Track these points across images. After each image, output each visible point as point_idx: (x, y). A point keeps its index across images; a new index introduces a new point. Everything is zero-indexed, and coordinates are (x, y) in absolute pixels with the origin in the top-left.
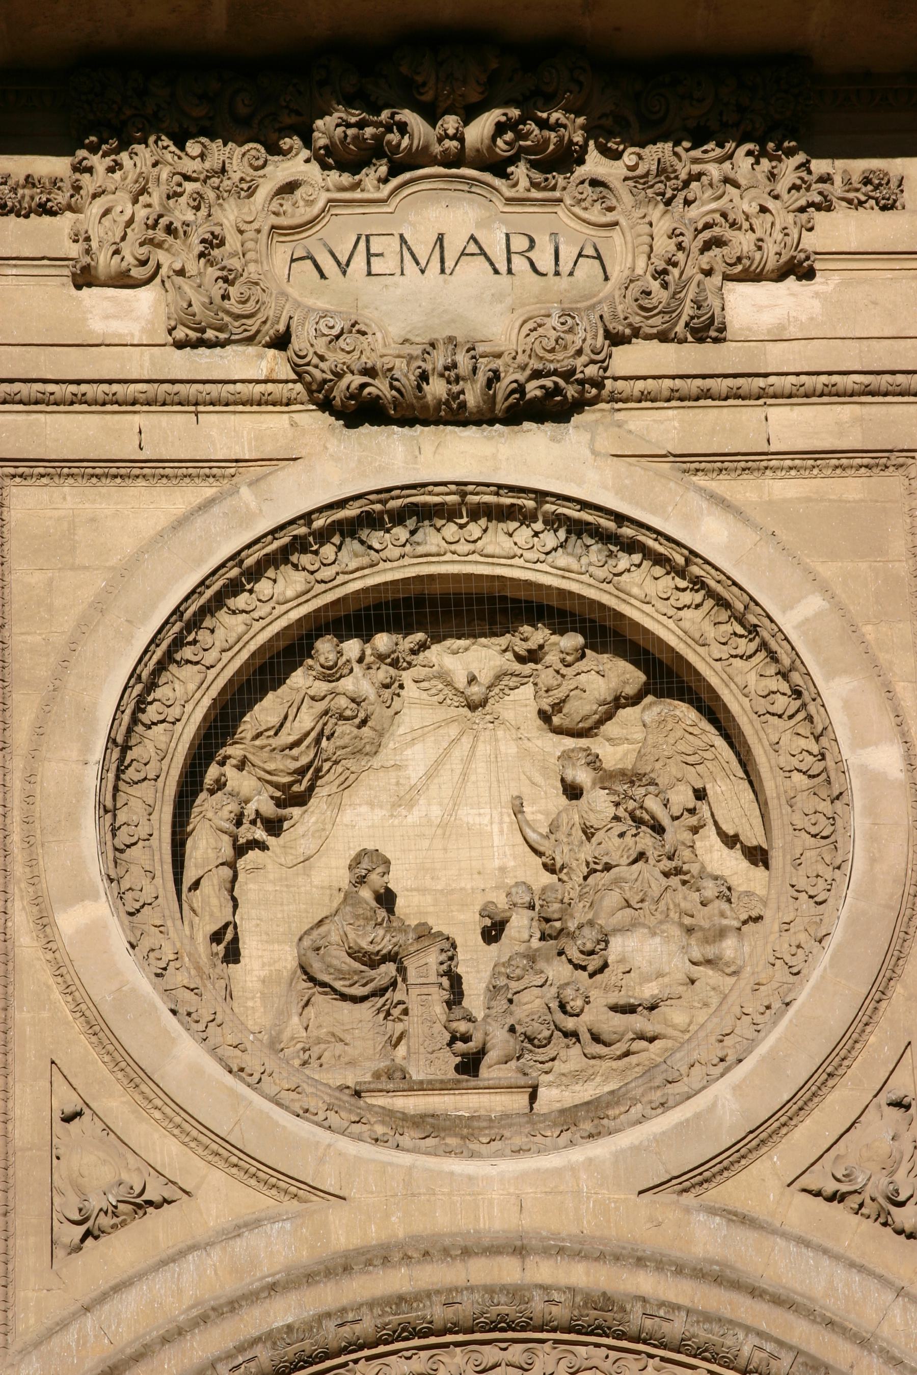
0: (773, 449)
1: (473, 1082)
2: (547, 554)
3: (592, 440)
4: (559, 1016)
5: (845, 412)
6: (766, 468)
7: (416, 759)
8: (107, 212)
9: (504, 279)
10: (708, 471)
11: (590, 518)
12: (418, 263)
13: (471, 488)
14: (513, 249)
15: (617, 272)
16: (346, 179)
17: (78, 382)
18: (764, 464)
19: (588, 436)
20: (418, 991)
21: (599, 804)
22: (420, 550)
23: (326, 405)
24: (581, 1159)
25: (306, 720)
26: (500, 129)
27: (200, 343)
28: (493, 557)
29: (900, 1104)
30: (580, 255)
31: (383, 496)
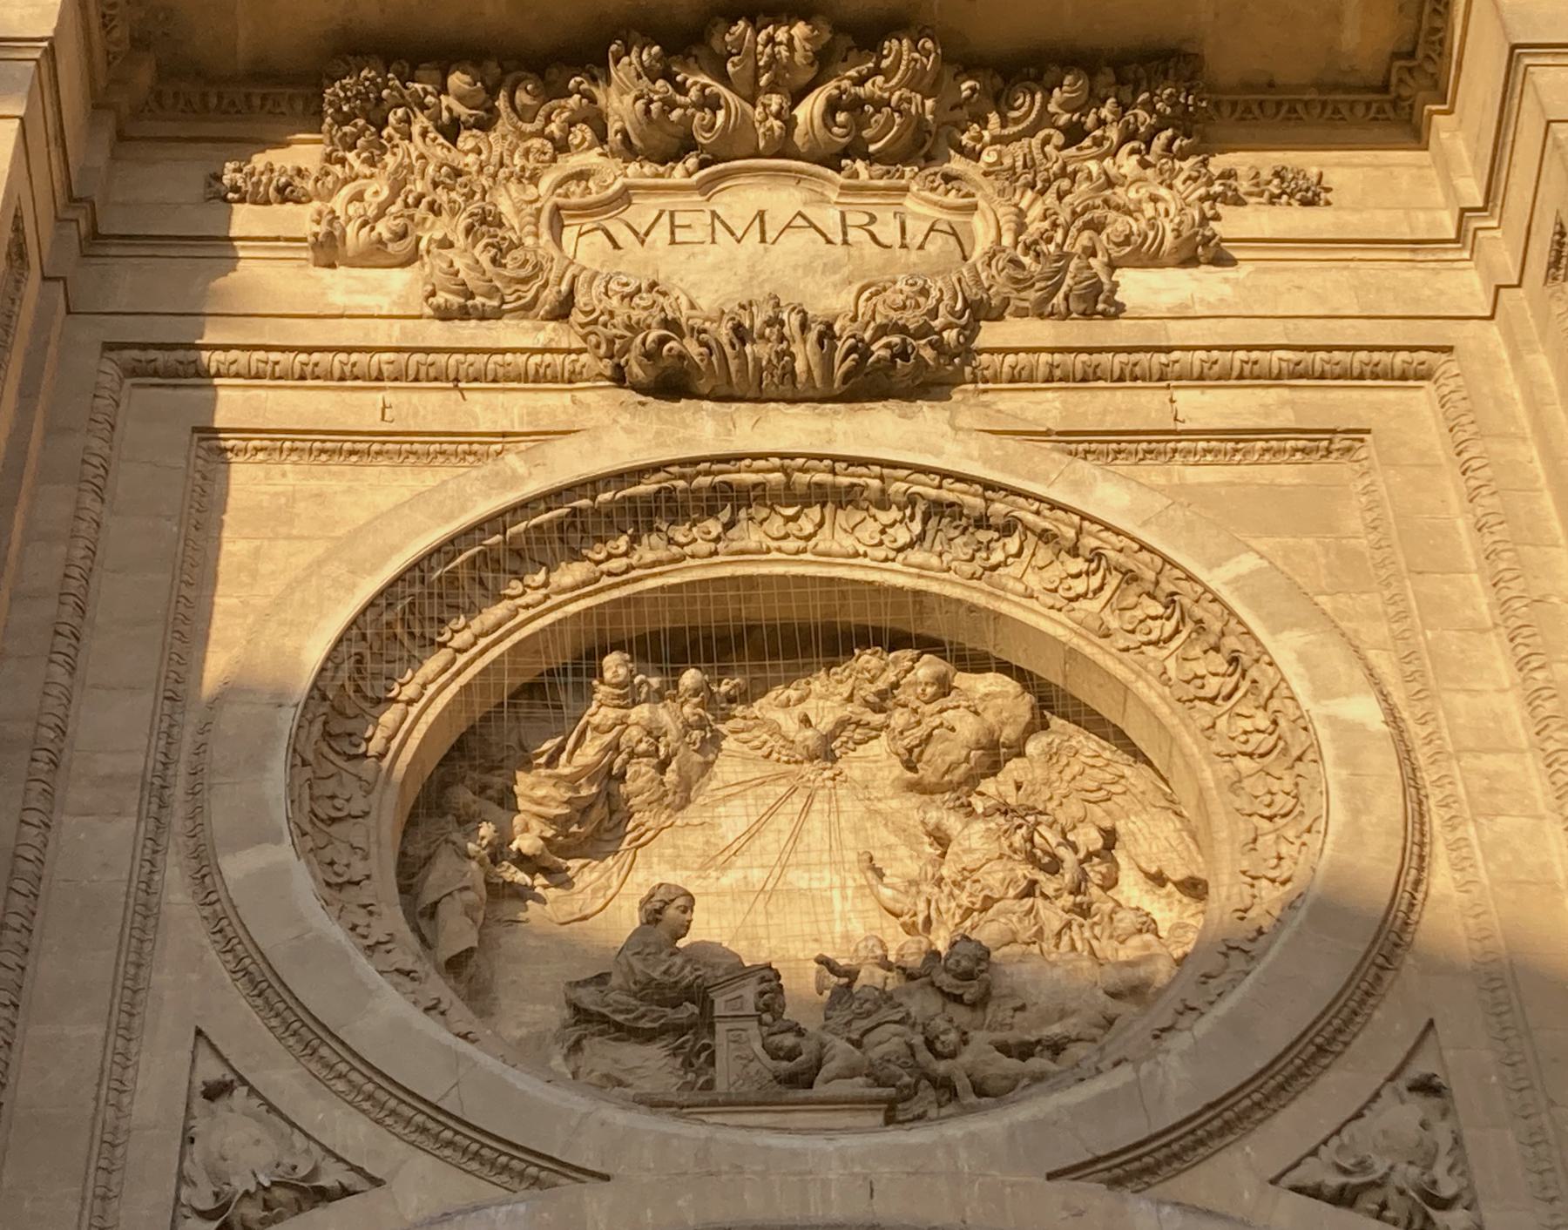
0: (1180, 427)
1: (802, 1094)
2: (900, 550)
3: (952, 416)
4: (924, 1056)
5: (1272, 396)
6: (1175, 451)
7: (733, 820)
8: (358, 197)
9: (839, 251)
10: (1101, 453)
11: (951, 497)
12: (732, 234)
13: (800, 461)
14: (848, 222)
15: (977, 255)
16: (649, 168)
17: (309, 350)
18: (1172, 445)
19: (947, 414)
20: (728, 1026)
21: (974, 839)
22: (736, 546)
23: (619, 378)
24: (959, 1134)
25: (589, 753)
26: (832, 107)
27: (464, 314)
28: (829, 555)
29: (1427, 1087)
30: (931, 229)
31: (687, 470)
